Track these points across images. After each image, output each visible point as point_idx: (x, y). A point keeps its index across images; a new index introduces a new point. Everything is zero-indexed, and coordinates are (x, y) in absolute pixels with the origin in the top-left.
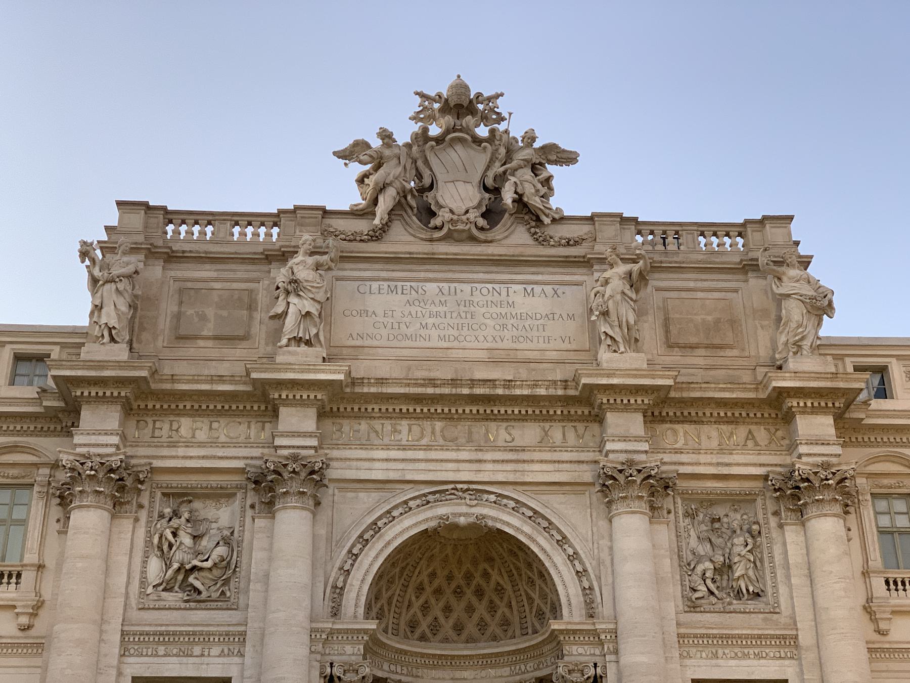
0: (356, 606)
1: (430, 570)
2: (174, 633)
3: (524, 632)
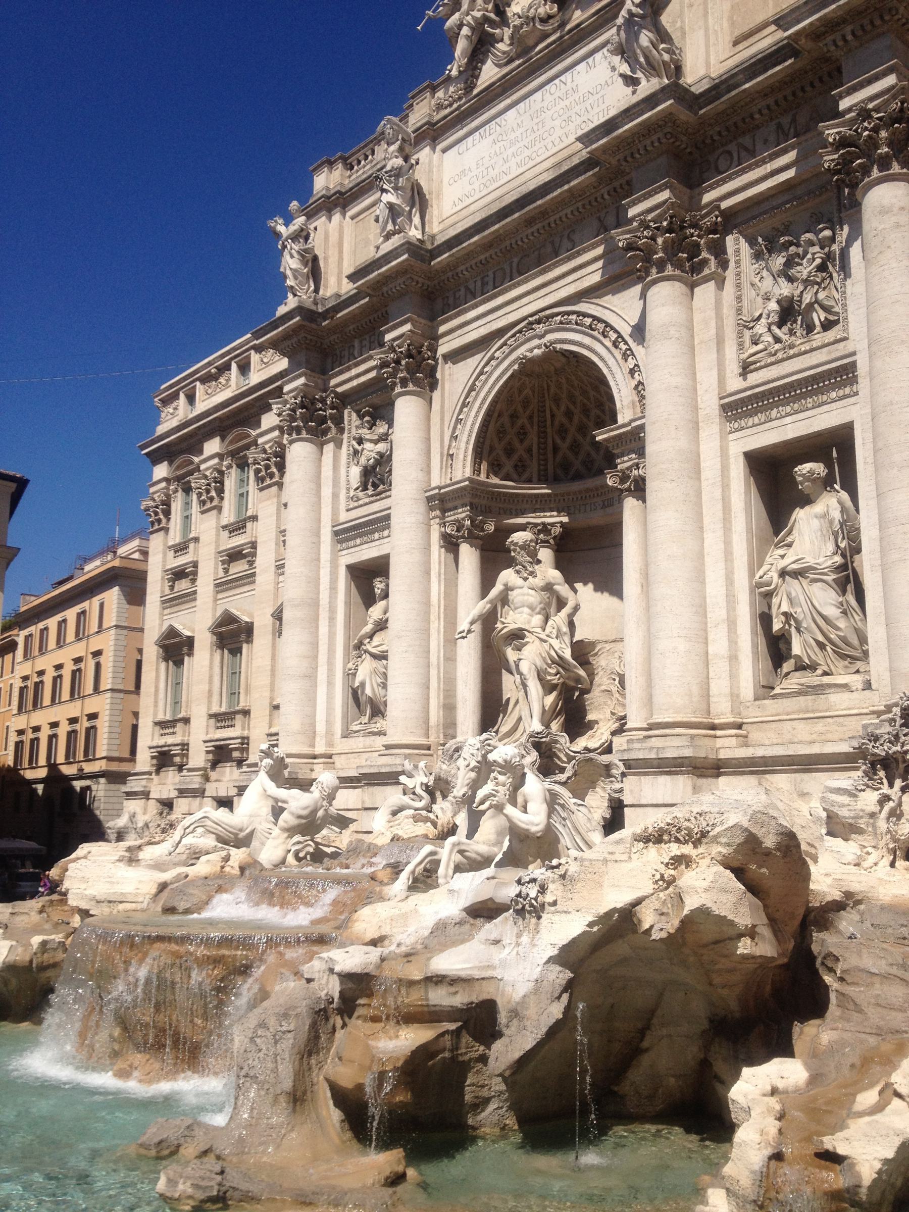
1: (563, 408)
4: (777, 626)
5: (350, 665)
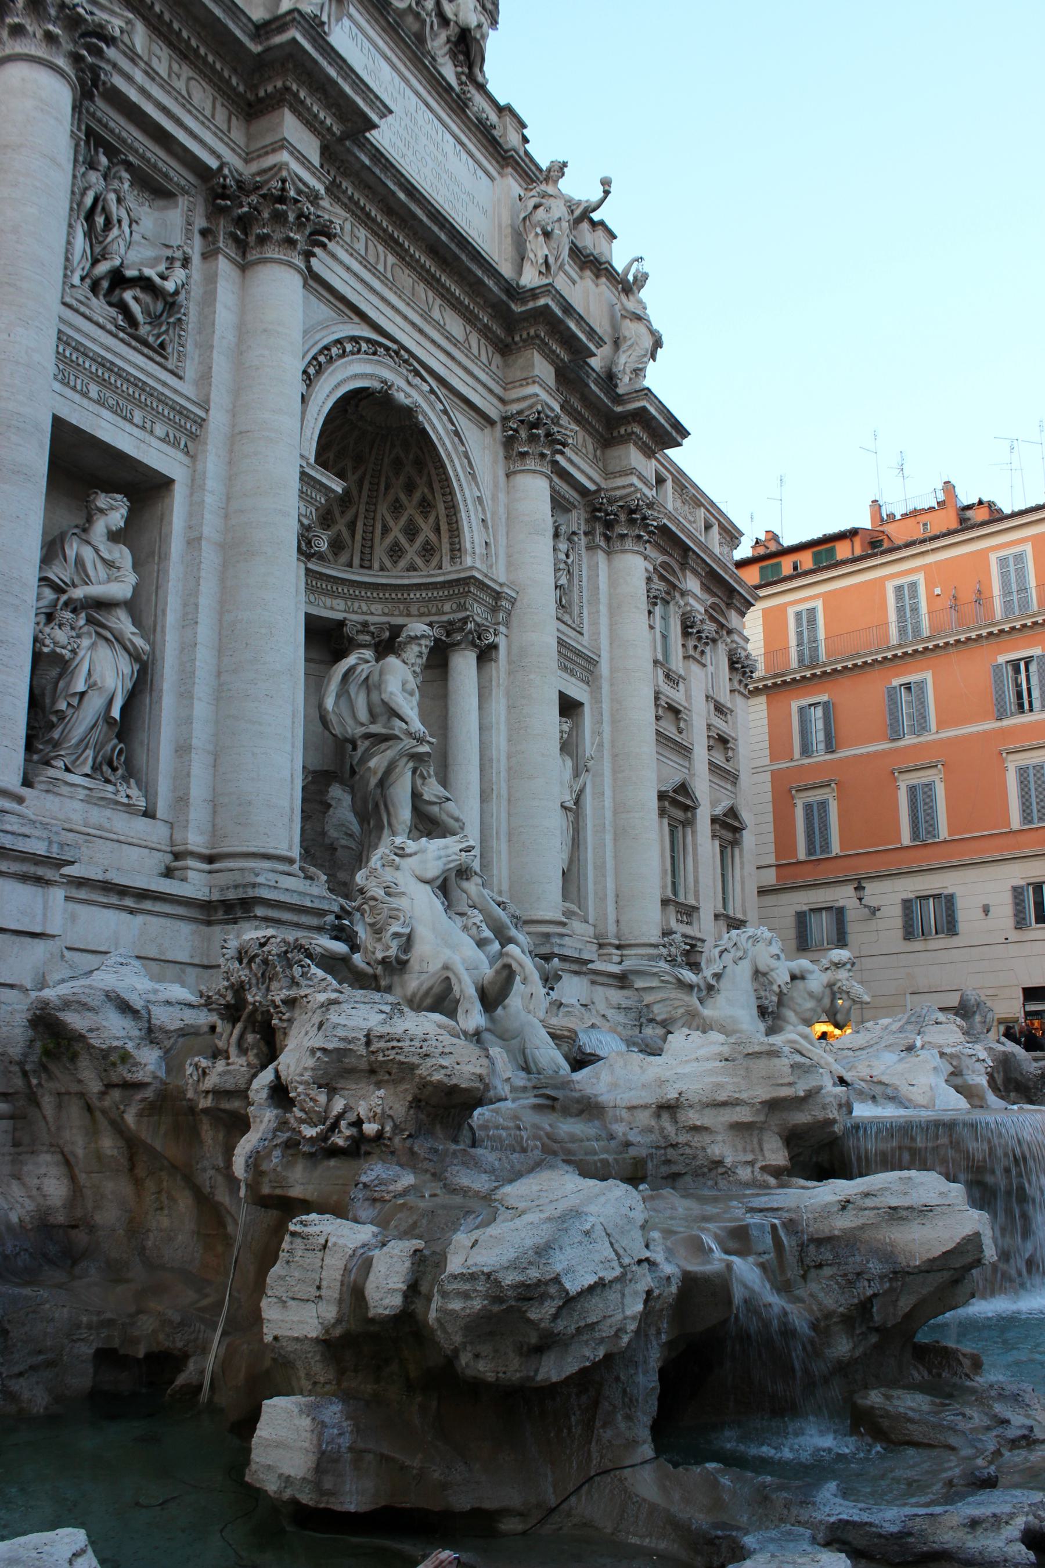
2: (120, 373)
3: (367, 564)
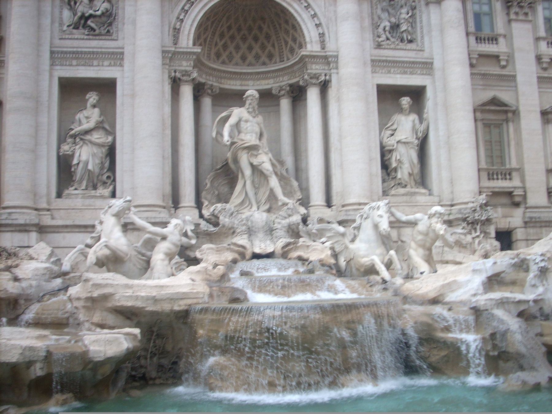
0: (188, 39)
1: (228, 24)
2: (82, 53)
3: (282, 60)
4: (394, 165)
5: (65, 148)
